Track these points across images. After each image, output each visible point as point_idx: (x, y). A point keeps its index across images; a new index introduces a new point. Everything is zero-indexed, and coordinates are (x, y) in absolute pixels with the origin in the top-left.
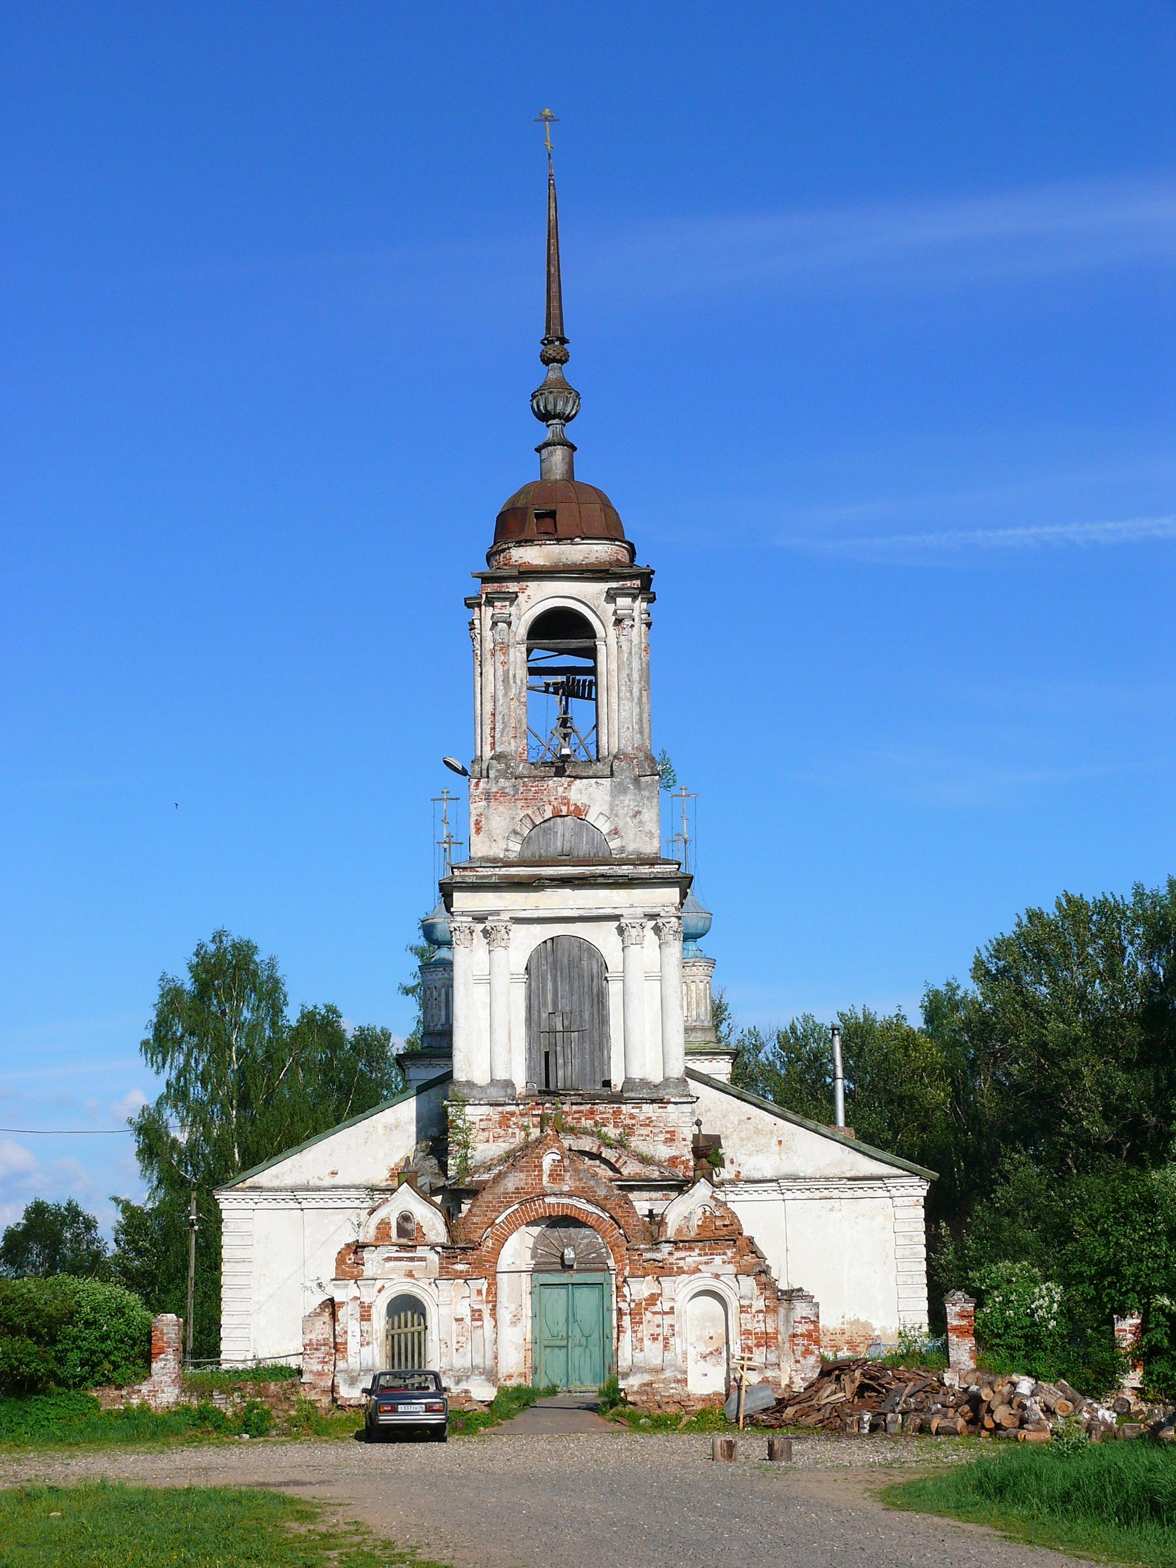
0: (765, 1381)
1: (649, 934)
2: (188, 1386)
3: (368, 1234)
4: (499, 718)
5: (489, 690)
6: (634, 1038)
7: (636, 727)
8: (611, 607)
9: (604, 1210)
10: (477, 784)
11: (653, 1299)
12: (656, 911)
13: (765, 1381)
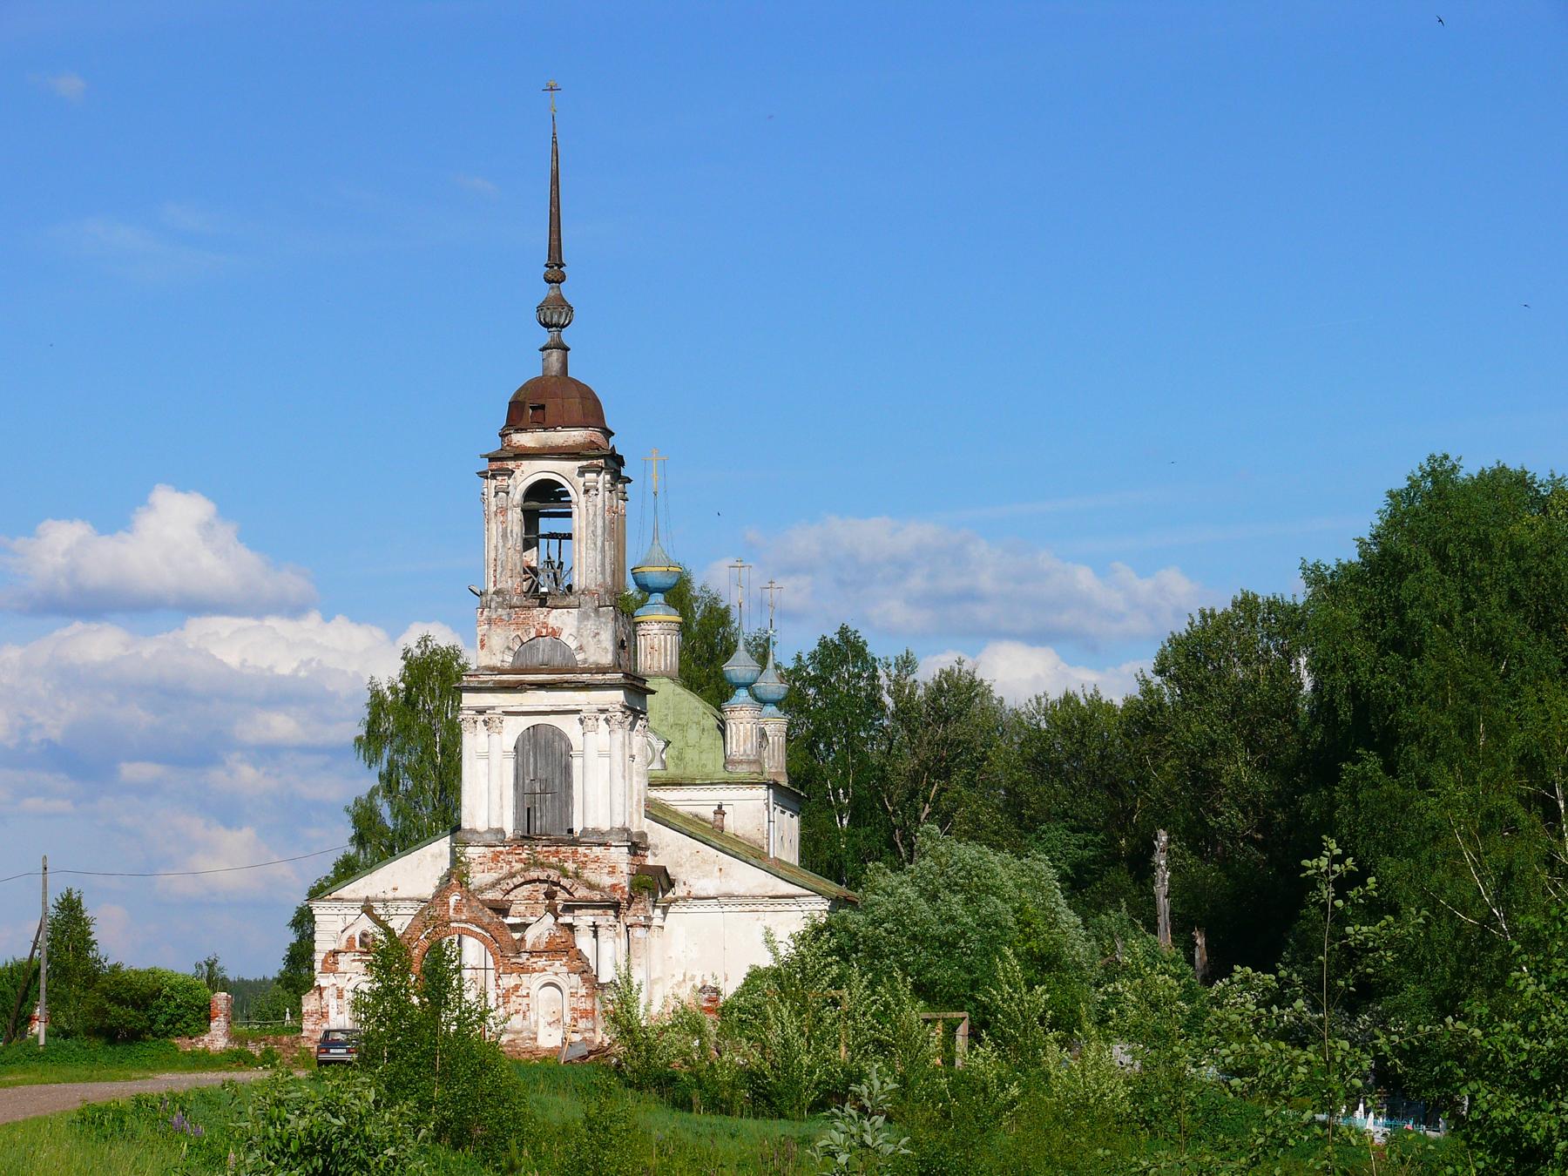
1: (602, 723)
2: (233, 1037)
3: (342, 945)
5: (493, 541)
6: (590, 798)
8: (582, 480)
11: (517, 987)
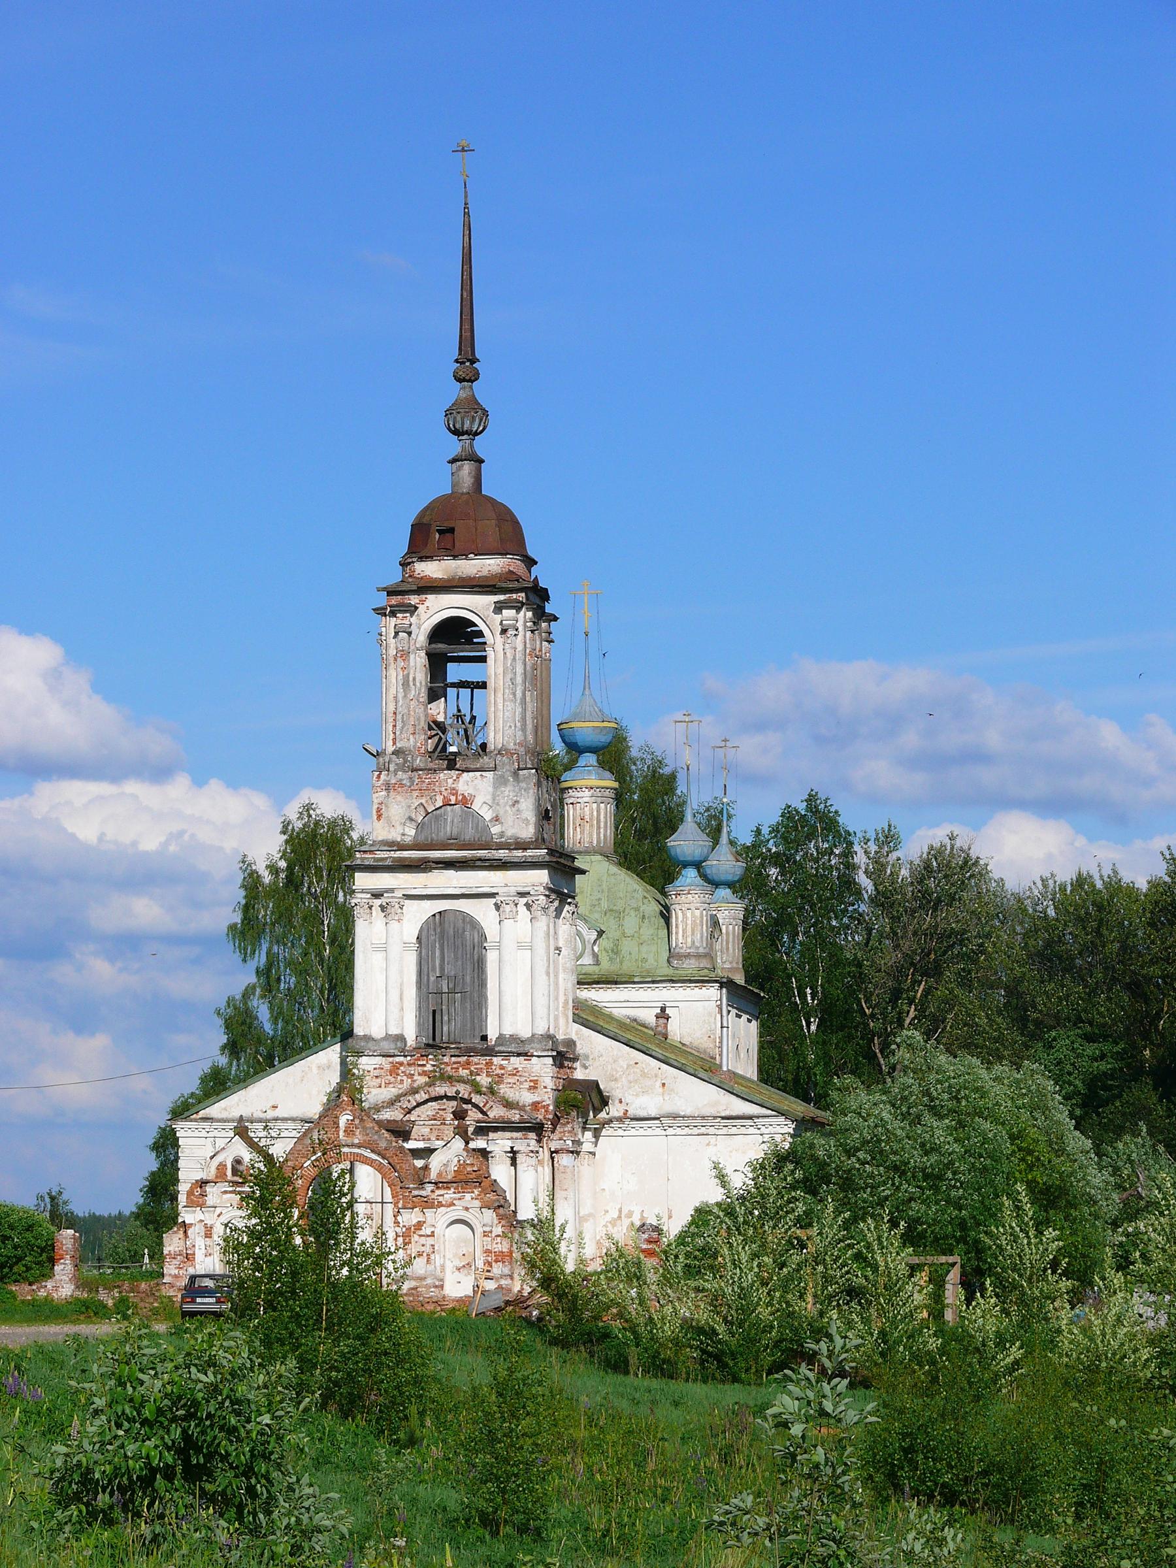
0: (500, 1287)
1: (522, 909)
2: (81, 1283)
3: (211, 1173)
4: (399, 717)
5: (393, 691)
6: (507, 999)
7: (518, 724)
8: (498, 618)
9: (384, 1158)
10: (379, 777)
11: (419, 1225)
12: (527, 889)
13: (500, 1287)
